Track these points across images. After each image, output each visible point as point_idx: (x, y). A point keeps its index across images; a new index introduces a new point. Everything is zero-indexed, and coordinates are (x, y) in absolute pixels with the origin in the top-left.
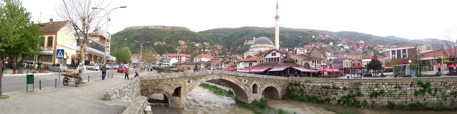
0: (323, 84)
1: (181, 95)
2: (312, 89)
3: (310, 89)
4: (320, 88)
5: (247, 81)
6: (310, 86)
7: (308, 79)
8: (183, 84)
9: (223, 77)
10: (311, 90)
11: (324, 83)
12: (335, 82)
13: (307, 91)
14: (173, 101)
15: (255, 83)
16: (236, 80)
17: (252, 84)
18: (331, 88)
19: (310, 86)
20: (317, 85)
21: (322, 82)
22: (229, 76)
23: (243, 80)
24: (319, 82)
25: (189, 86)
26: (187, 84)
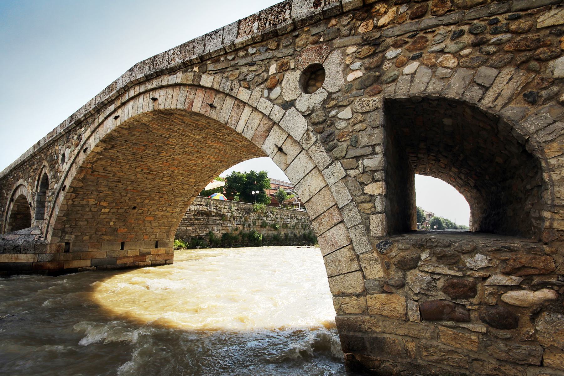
0: (201, 208)
11: (201, 205)
12: (219, 206)
18: (213, 214)
21: (198, 203)
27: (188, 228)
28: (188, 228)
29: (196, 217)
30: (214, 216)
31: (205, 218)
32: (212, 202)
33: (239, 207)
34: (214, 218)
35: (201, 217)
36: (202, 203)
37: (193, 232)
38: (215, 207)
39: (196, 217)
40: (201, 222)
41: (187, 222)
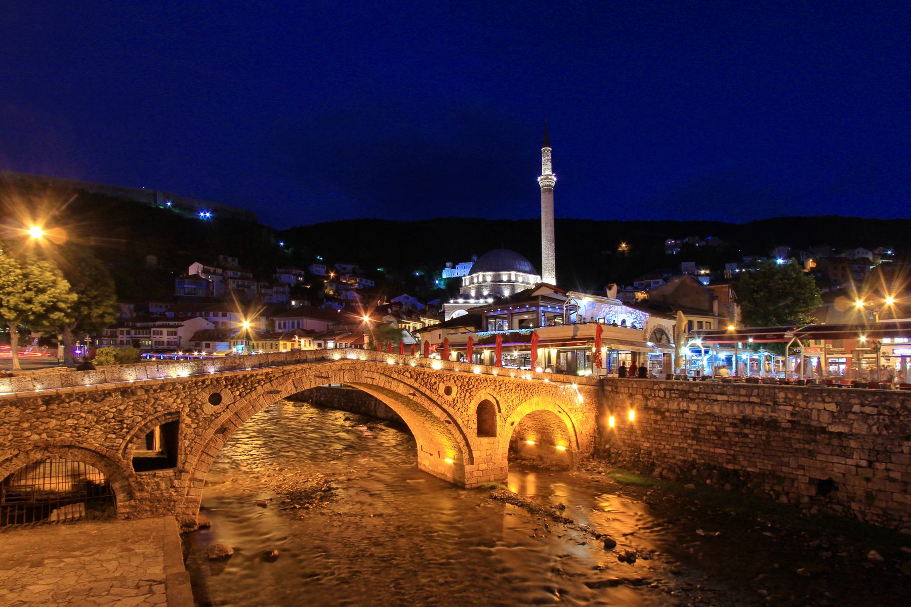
1: (181, 458)
2: (695, 427)
3: (690, 426)
4: (734, 425)
5: (455, 390)
6: (686, 415)
7: (680, 387)
8: (187, 410)
9: (365, 374)
10: (694, 430)
13: (674, 433)
14: (142, 490)
15: (483, 398)
16: (416, 385)
17: (473, 402)
19: (687, 411)
20: (716, 409)
21: (742, 399)
22: (388, 373)
23: (442, 388)
24: (725, 398)
25: (217, 415)
26: (209, 409)
27: (718, 451)
28: (718, 451)
29: (737, 430)
30: (784, 430)
31: (760, 433)
32: (782, 395)
33: (885, 407)
34: (787, 434)
35: (747, 431)
36: (753, 399)
37: (729, 462)
38: (790, 408)
39: (737, 430)
40: (748, 440)
41: (715, 438)
